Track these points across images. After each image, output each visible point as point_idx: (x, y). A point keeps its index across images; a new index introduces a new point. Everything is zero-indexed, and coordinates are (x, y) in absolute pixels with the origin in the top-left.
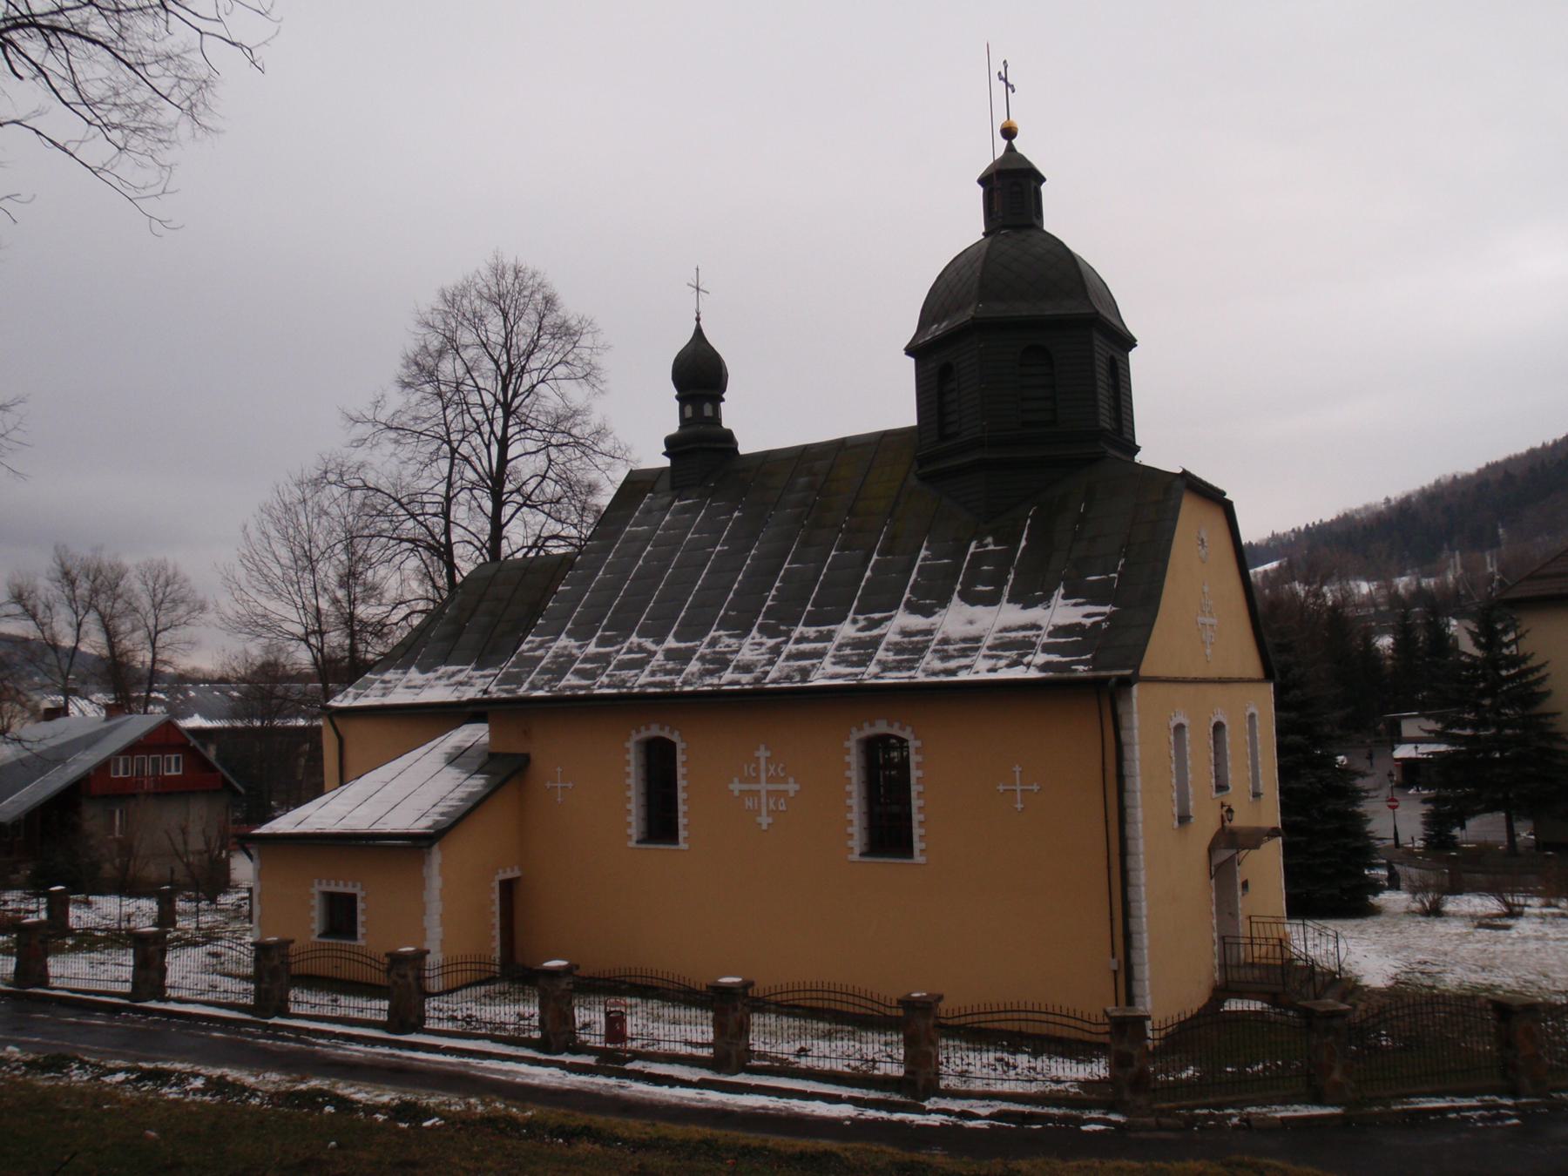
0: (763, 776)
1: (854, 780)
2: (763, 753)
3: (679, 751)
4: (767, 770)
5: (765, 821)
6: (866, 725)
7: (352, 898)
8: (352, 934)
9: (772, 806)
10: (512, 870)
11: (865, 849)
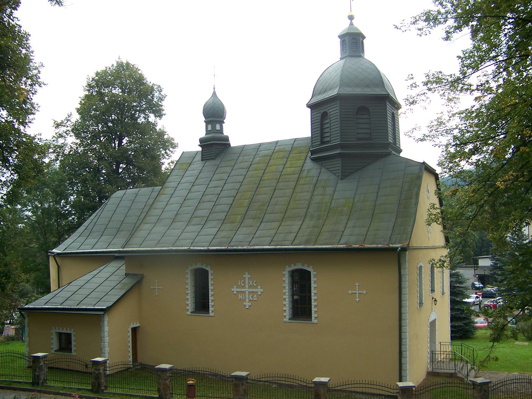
0: (247, 286)
1: (287, 288)
2: (247, 276)
3: (210, 274)
4: (249, 283)
5: (247, 304)
6: (293, 265)
7: (69, 336)
8: (70, 350)
9: (251, 298)
10: (136, 323)
11: (291, 316)
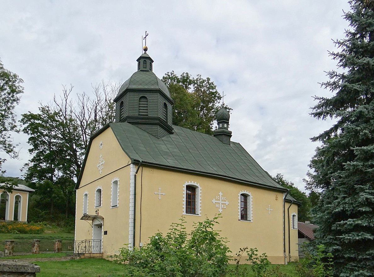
2: (221, 194)
9: (222, 207)
